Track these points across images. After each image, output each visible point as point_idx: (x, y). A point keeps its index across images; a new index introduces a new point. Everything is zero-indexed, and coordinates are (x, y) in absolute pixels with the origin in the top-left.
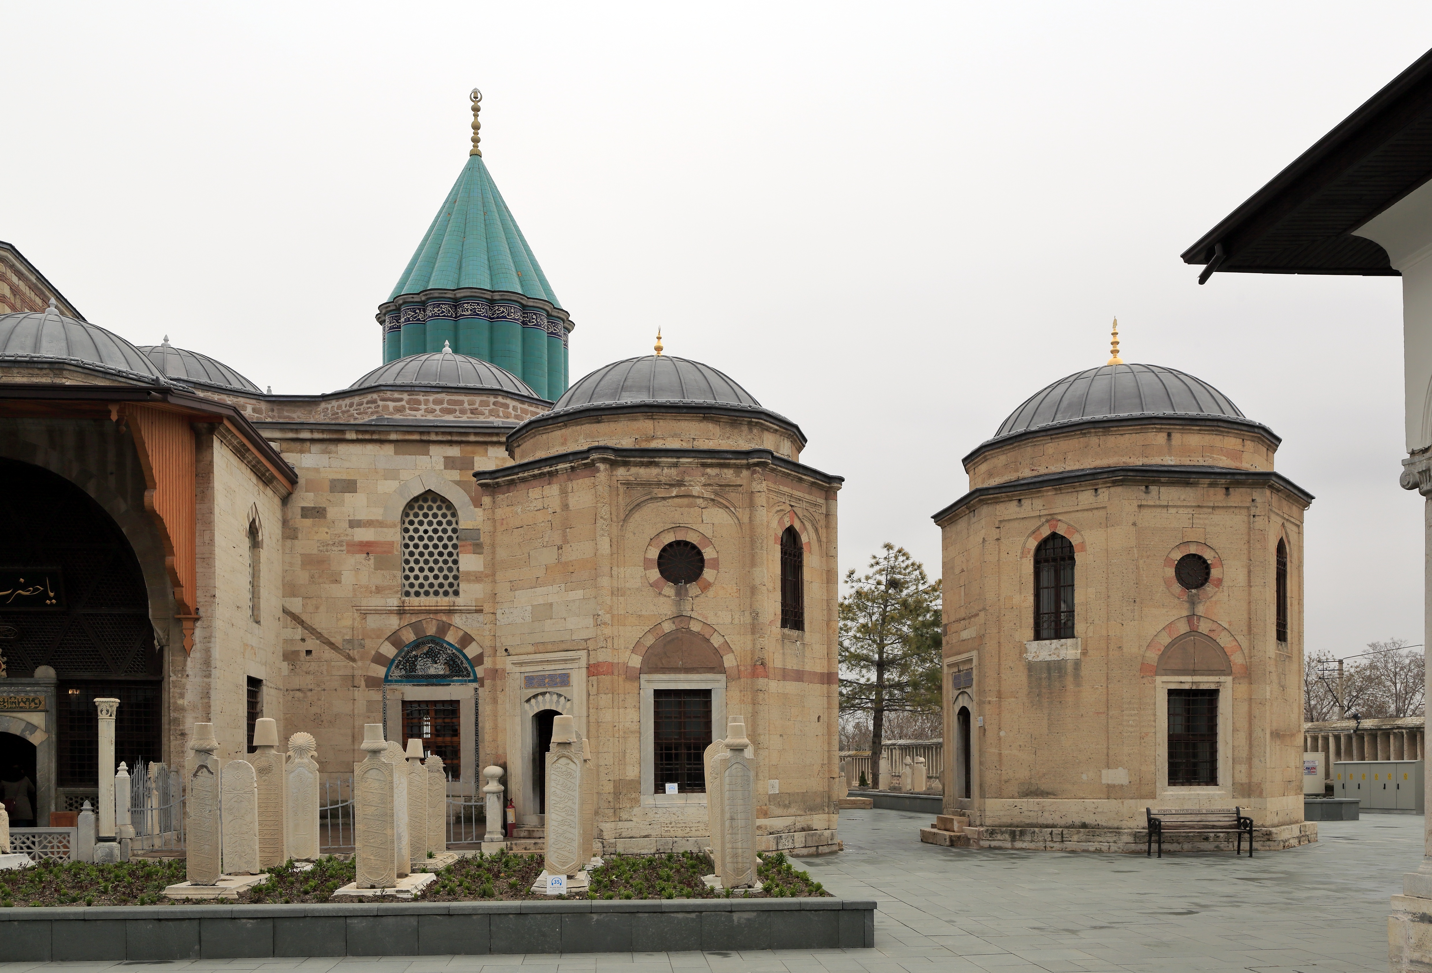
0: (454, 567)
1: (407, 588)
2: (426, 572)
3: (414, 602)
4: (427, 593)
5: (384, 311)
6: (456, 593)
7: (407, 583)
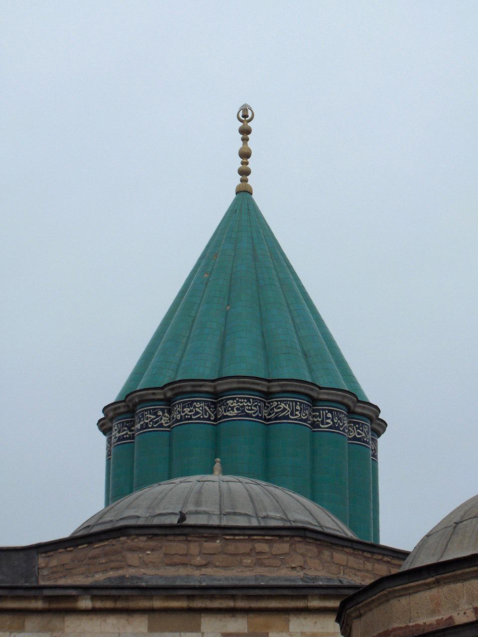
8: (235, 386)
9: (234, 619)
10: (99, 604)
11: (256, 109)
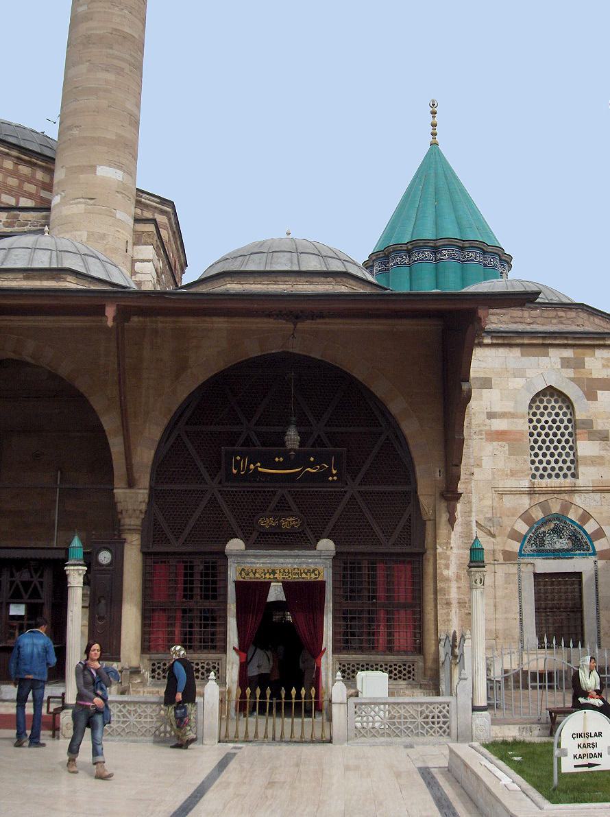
0: (571, 452)
1: (534, 472)
2: (548, 457)
3: (546, 483)
4: (550, 476)
5: (374, 258)
6: (574, 476)
7: (533, 467)
8: (446, 243)
9: (565, 350)
10: (495, 341)
11: (438, 101)
